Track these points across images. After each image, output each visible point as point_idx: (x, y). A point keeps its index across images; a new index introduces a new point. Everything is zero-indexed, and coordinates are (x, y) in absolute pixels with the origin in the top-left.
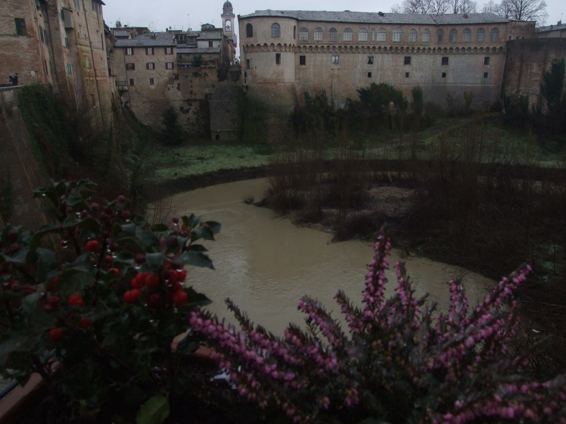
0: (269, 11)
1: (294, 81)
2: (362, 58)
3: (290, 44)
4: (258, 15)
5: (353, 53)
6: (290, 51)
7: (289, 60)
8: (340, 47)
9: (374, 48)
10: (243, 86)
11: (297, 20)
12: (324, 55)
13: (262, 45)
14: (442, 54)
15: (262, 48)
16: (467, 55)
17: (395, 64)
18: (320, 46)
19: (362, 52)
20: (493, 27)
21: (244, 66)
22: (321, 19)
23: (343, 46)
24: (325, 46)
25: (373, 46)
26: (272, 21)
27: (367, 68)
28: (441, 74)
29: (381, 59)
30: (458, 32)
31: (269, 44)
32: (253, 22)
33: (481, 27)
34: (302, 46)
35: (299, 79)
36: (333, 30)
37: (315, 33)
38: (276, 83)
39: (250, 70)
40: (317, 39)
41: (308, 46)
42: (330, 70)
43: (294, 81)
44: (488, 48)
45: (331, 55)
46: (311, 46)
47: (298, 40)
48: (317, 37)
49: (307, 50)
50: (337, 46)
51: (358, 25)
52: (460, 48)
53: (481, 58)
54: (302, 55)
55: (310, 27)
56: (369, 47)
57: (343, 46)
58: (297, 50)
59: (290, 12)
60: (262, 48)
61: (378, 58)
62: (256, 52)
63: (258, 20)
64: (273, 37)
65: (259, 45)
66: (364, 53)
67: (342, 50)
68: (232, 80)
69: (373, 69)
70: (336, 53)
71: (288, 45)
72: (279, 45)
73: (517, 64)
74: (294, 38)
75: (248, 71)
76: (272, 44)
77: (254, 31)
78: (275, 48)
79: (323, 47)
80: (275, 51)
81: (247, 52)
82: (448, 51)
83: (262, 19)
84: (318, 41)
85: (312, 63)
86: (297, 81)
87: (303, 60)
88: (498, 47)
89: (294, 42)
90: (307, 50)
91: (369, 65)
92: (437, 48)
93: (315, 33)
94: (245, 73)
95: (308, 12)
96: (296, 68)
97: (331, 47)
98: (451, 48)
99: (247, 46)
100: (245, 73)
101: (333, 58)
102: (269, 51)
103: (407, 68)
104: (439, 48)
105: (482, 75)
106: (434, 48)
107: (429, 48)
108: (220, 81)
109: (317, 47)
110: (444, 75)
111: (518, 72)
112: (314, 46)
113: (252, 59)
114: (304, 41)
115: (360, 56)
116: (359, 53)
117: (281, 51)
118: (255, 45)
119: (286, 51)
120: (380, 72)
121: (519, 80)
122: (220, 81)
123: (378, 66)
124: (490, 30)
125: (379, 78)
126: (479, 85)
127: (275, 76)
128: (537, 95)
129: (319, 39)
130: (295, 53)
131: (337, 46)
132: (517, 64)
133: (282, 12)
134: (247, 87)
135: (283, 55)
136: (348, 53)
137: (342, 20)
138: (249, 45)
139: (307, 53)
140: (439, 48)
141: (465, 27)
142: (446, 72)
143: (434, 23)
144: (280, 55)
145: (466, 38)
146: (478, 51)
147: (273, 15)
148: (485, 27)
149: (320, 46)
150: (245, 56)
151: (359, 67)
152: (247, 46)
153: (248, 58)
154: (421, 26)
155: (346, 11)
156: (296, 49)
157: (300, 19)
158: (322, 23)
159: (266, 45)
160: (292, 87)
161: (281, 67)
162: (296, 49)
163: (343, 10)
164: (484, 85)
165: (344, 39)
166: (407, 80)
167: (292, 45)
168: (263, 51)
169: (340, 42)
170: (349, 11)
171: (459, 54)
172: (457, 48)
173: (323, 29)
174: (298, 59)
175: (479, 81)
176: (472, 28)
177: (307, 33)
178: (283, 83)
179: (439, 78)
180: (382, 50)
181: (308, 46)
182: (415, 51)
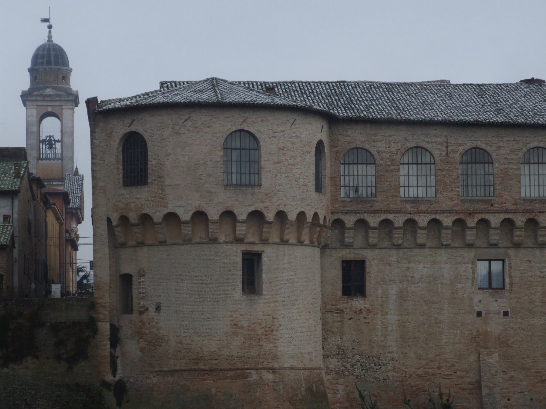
0: (214, 83)
1: (319, 362)
3: (301, 215)
4: (171, 98)
6: (300, 243)
7: (298, 275)
8: (508, 223)
10: (105, 384)
11: (331, 119)
12: (443, 255)
13: (185, 216)
15: (187, 230)
18: (423, 220)
21: (108, 299)
22: (428, 115)
23: (520, 220)
24: (447, 221)
26: (227, 123)
31: (214, 214)
32: (146, 126)
34: (349, 220)
35: (341, 353)
36: (477, 157)
37: (403, 170)
38: (241, 373)
39: (134, 317)
40: (413, 193)
41: (374, 221)
43: (319, 362)
45: (470, 254)
46: (386, 223)
47: (335, 198)
48: (413, 184)
49: (373, 237)
50: (495, 220)
54: (349, 255)
55: (381, 146)
57: (520, 220)
58: (330, 235)
59: (301, 87)
60: (187, 230)
62: (163, 243)
63: (167, 119)
64: (228, 185)
65: (171, 217)
67: (519, 235)
68: (58, 358)
70: (494, 246)
71: (292, 216)
72: (257, 216)
74: (318, 189)
75: (127, 324)
76: (229, 215)
77: (152, 162)
78: (241, 229)
79: (435, 222)
80: (240, 241)
81: (123, 245)
83: (185, 114)
84: (416, 201)
85: (393, 290)
86: (334, 363)
87: (354, 278)
89: (317, 205)
90: (373, 237)
93: (403, 170)
94: (115, 330)
95: (372, 87)
96: (325, 311)
97: (472, 222)
99: (124, 219)
100: (115, 330)
101: (482, 267)
102: (214, 241)
109: (411, 223)
112: (399, 221)
113: (142, 274)
114: (358, 200)
117: (264, 241)
118: (158, 217)
119: (284, 242)
129: (421, 193)
130: (324, 248)
131: (495, 220)
133: (269, 88)
134: (120, 389)
135: (273, 258)
137: (514, 117)
138: (133, 217)
139: (373, 247)
144: (258, 255)
147: (232, 98)
149: (423, 220)
152: (124, 219)
153: (127, 269)
156: (324, 232)
157: (342, 113)
158: (432, 131)
159: (200, 216)
160: (309, 389)
161: (261, 307)
162: (324, 232)
163: (515, 79)
165: (525, 193)
167: (309, 217)
168: (188, 241)
169: (509, 206)
170: (540, 82)
174: (335, 273)
177: (371, 170)
178: (273, 370)
181: (374, 221)
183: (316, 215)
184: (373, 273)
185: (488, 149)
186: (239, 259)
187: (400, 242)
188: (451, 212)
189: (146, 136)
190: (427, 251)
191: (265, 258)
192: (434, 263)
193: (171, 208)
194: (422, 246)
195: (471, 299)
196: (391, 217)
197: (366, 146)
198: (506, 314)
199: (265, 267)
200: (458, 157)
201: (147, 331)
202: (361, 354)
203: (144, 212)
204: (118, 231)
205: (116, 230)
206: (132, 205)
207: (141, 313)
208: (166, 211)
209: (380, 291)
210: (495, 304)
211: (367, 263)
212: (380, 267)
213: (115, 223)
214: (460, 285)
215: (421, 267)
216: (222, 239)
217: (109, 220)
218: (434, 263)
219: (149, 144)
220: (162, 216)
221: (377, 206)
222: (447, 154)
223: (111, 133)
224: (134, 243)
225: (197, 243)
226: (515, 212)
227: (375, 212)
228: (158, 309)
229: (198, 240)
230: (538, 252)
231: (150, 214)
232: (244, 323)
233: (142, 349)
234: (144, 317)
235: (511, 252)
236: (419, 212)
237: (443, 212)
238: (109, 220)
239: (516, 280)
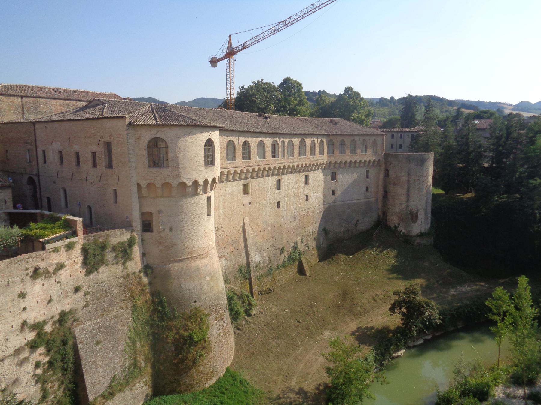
16: (352, 169)
25: (283, 164)
28: (331, 192)
42: (242, 206)
73: (404, 178)
91: (278, 191)
105: (365, 189)
108: (89, 273)
111: (406, 187)
113: (160, 212)
115: (270, 178)
118: (175, 183)
121: (408, 195)
122: (89, 273)
126: (363, 201)
132: (404, 178)
138: (159, 183)
143: (325, 133)
150: (141, 206)
151: (269, 196)
153: (147, 210)
159: (196, 183)
166: (306, 203)
169: (255, 164)
201: (164, 241)
203: (166, 181)
204: (144, 192)
208: (180, 181)
213: (142, 186)
217: (138, 185)
220: (177, 183)
223: (140, 137)
228: (171, 230)
233: (161, 251)
234: (162, 234)
238: (138, 185)
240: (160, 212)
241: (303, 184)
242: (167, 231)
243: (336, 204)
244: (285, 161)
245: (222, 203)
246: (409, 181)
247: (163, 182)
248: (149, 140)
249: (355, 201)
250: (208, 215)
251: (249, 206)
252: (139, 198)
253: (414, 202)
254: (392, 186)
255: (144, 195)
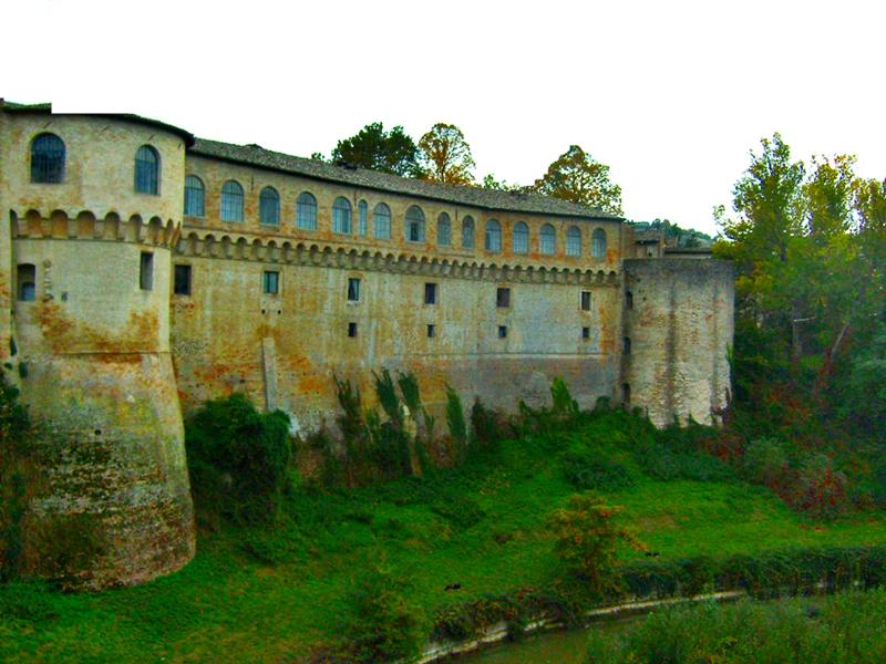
2: (336, 280)
5: (316, 265)
9: (366, 254)
12: (243, 266)
13: (100, 214)
14: (496, 280)
15: (99, 228)
16: (548, 286)
17: (405, 300)
19: (335, 263)
20: (597, 225)
23: (294, 244)
24: (250, 240)
25: (364, 248)
26: (138, 138)
27: (346, 311)
29: (374, 288)
30: (531, 231)
31: (125, 216)
32: (65, 132)
33: (574, 223)
36: (269, 198)
39: (37, 304)
41: (202, 235)
42: (260, 313)
44: (589, 272)
49: (200, 248)
50: (279, 242)
51: (331, 187)
52: (537, 267)
53: (576, 293)
54: (181, 260)
56: (353, 252)
57: (294, 244)
61: (371, 284)
65: (87, 216)
66: (341, 267)
69: (360, 311)
70: (275, 261)
72: (156, 221)
73: (663, 309)
76: (136, 218)
77: (69, 163)
79: (241, 240)
80: (140, 242)
81: (25, 237)
82: (511, 275)
85: (209, 291)
88: (607, 271)
90: (200, 248)
91: (350, 302)
92: (487, 266)
98: (518, 268)
99: (33, 214)
102: (120, 240)
103: (430, 315)
104: (493, 266)
106: (483, 265)
107: (474, 264)
109: (225, 239)
110: (503, 331)
112: (219, 237)
113: (47, 265)
115: (332, 273)
116: (329, 266)
117: (155, 244)
118: (73, 213)
120: (374, 322)
123: (371, 305)
124: (591, 232)
125: (372, 338)
126: (575, 357)
127: (136, 328)
128: (709, 379)
131: (279, 242)
136: (303, 264)
138: (45, 212)
139: (197, 255)
140: (493, 266)
141: (544, 221)
142: (508, 326)
145: (570, 249)
146: (570, 278)
148: (581, 224)
151: (328, 306)
152: (33, 214)
153: (26, 259)
154: (459, 208)
155: (255, 146)
159: (113, 217)
164: (583, 357)
166: (430, 343)
168: (98, 238)
169: (289, 233)
171: (533, 282)
172: (531, 268)
173: (246, 187)
175: (574, 348)
176: (557, 223)
179: (493, 340)
180: (382, 262)
182: (447, 271)
183: (170, 222)
184: (197, 275)
185: (277, 188)
186: (138, 257)
187: (217, 253)
188: (253, 234)
189: (63, 139)
190: (232, 262)
191: (155, 259)
192: (237, 271)
193: (87, 207)
194: (230, 258)
195: (259, 300)
196: (213, 233)
197: (200, 175)
198: (279, 312)
199: (154, 266)
200: (258, 192)
202: (186, 340)
203: (59, 208)
205: (19, 222)
206: (45, 201)
207: (45, 301)
208: (81, 209)
209: (200, 291)
210: (275, 305)
211: (193, 269)
212: (201, 271)
213: (20, 216)
214: (252, 290)
215: (228, 273)
216: (127, 240)
217: (13, 213)
218: (237, 271)
219: (68, 146)
221: (206, 224)
222: (252, 189)
224: (40, 236)
225: (106, 241)
226: (292, 238)
227: (202, 228)
228: (64, 297)
229: (106, 238)
230: (299, 268)
231: (66, 211)
232: (140, 314)
233: (45, 334)
235: (285, 267)
236: (232, 232)
237: (247, 233)
238: (13, 213)
239: (287, 287)
240: (47, 265)
241: (420, 301)
242: (58, 300)
243: (508, 356)
244: (367, 242)
245: (209, 297)
246: (672, 316)
247: (53, 209)
248: (33, 136)
249: (557, 357)
250: (142, 287)
251: (276, 316)
252: (13, 239)
253: (685, 360)
254: (639, 326)
255: (22, 233)
